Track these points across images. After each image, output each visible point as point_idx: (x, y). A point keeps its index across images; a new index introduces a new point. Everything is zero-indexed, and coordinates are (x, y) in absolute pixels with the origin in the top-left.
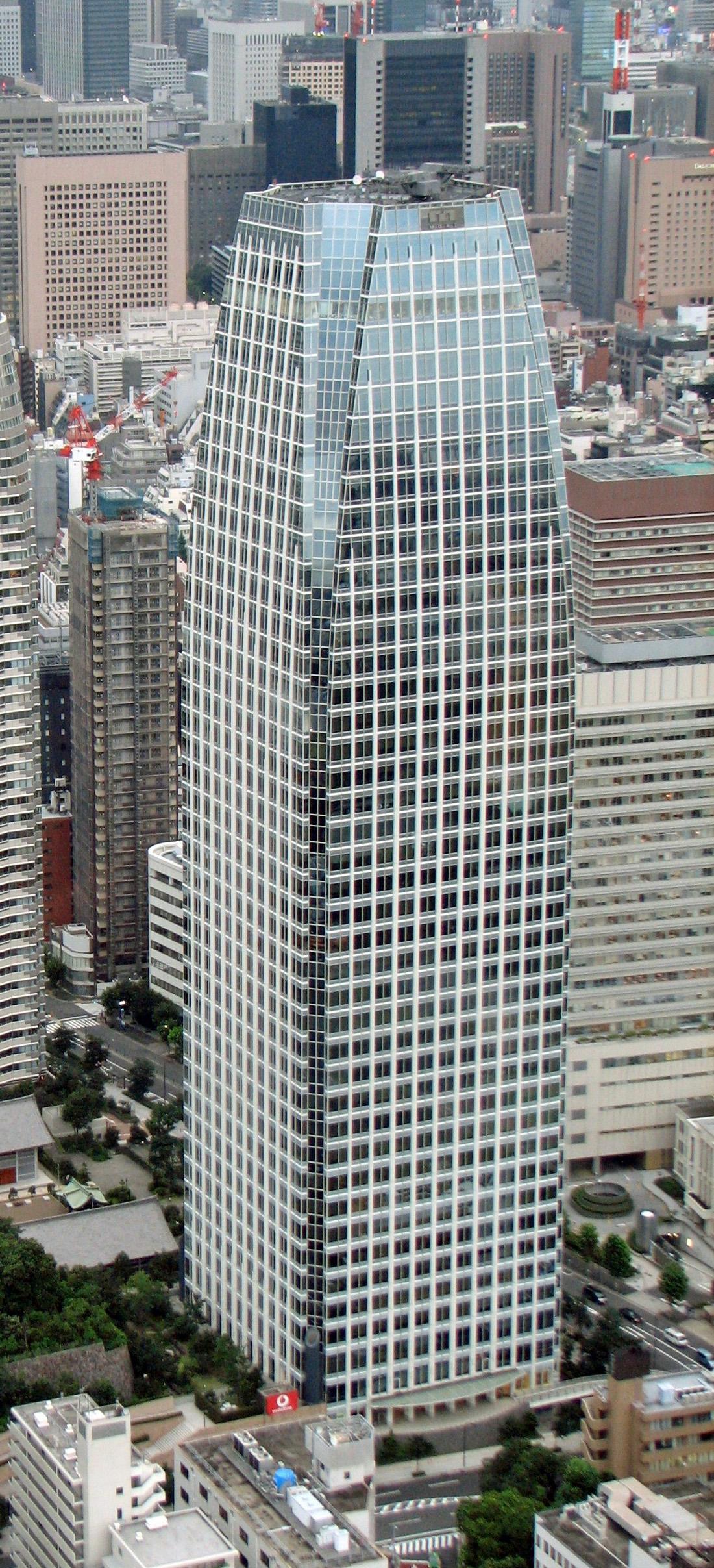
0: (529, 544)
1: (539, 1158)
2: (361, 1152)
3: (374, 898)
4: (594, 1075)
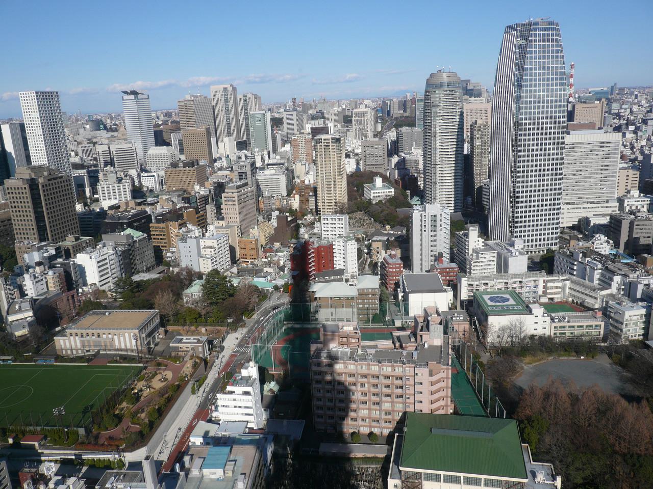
0: (558, 104)
1: (555, 226)
2: (522, 197)
3: (526, 164)
4: (566, 211)
